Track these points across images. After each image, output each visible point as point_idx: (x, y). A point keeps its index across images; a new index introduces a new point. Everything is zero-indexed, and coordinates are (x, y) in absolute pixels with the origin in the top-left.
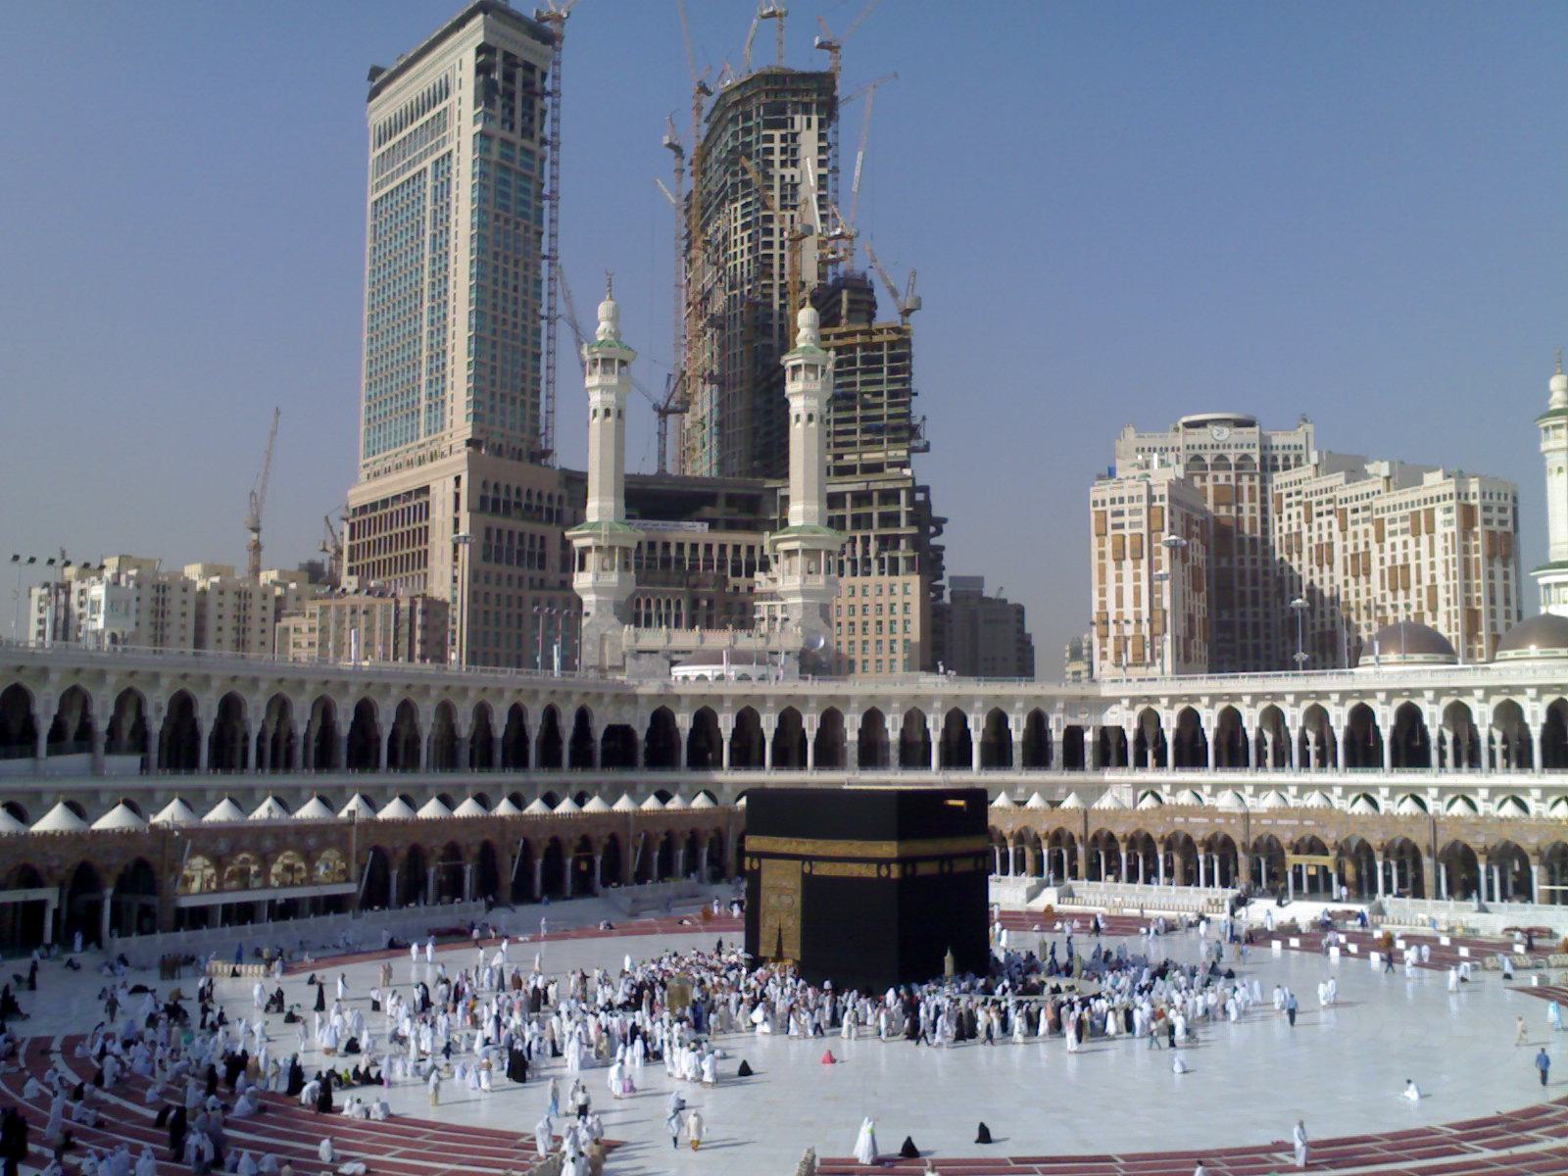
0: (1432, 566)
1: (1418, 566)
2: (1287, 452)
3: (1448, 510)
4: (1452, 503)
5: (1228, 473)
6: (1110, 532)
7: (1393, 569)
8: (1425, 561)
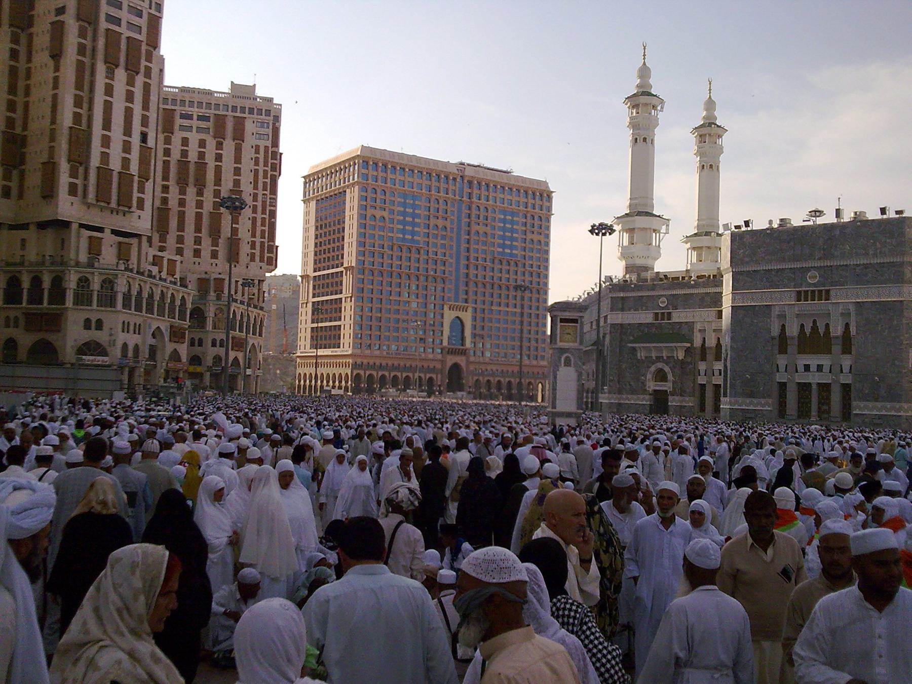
0: (237, 171)
1: (218, 170)
6: (103, 25)
7: (183, 164)
8: (228, 164)
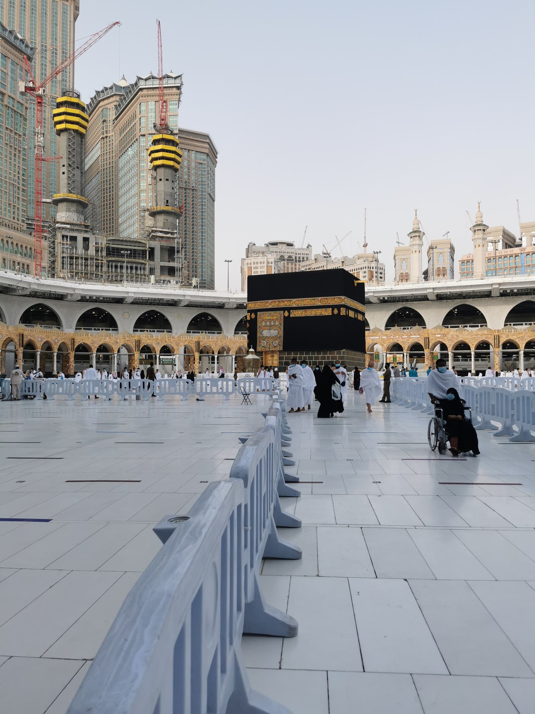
2: (303, 256)
3: (365, 272)
4: (367, 270)
5: (284, 262)
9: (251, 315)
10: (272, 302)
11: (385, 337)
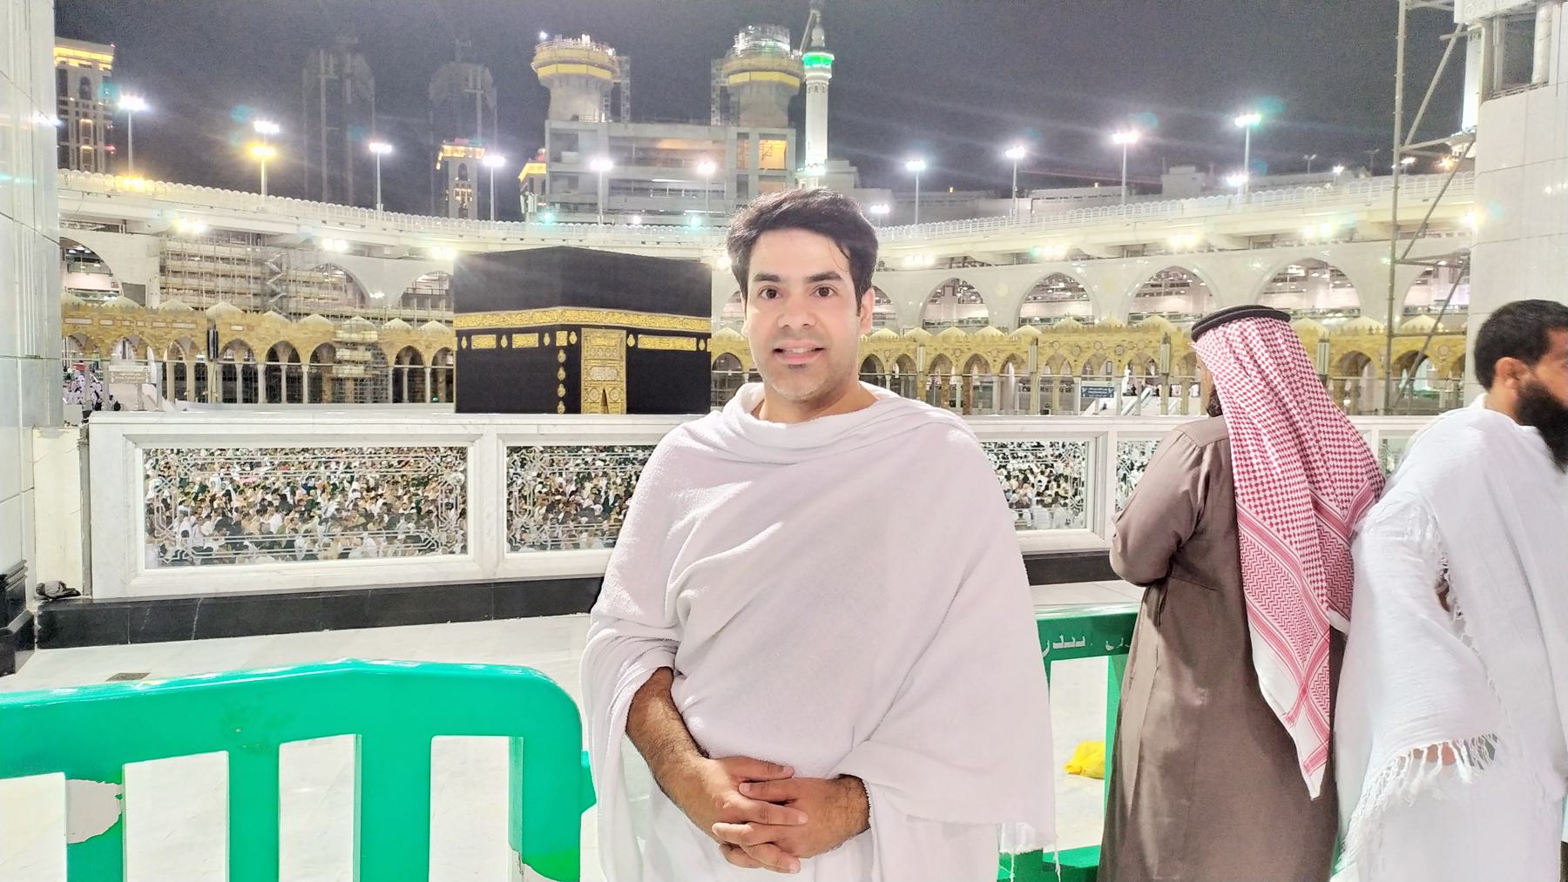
9: (569, 335)
10: (607, 315)
11: (110, 322)
